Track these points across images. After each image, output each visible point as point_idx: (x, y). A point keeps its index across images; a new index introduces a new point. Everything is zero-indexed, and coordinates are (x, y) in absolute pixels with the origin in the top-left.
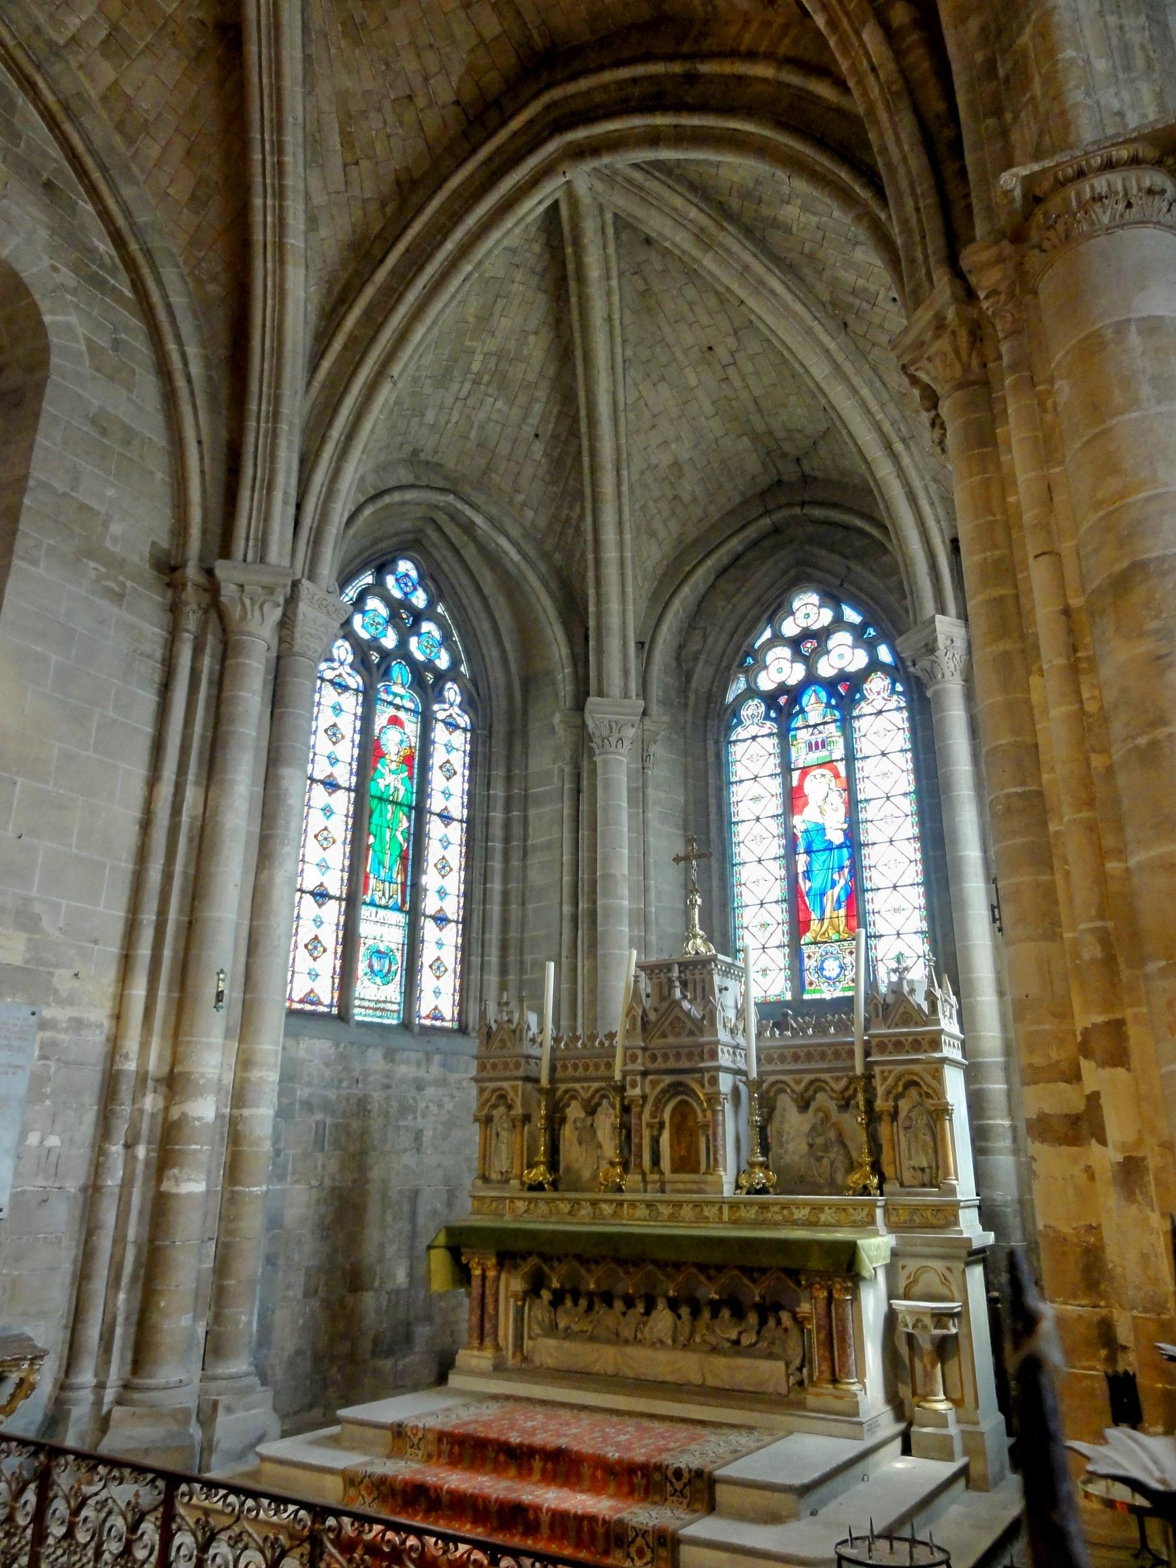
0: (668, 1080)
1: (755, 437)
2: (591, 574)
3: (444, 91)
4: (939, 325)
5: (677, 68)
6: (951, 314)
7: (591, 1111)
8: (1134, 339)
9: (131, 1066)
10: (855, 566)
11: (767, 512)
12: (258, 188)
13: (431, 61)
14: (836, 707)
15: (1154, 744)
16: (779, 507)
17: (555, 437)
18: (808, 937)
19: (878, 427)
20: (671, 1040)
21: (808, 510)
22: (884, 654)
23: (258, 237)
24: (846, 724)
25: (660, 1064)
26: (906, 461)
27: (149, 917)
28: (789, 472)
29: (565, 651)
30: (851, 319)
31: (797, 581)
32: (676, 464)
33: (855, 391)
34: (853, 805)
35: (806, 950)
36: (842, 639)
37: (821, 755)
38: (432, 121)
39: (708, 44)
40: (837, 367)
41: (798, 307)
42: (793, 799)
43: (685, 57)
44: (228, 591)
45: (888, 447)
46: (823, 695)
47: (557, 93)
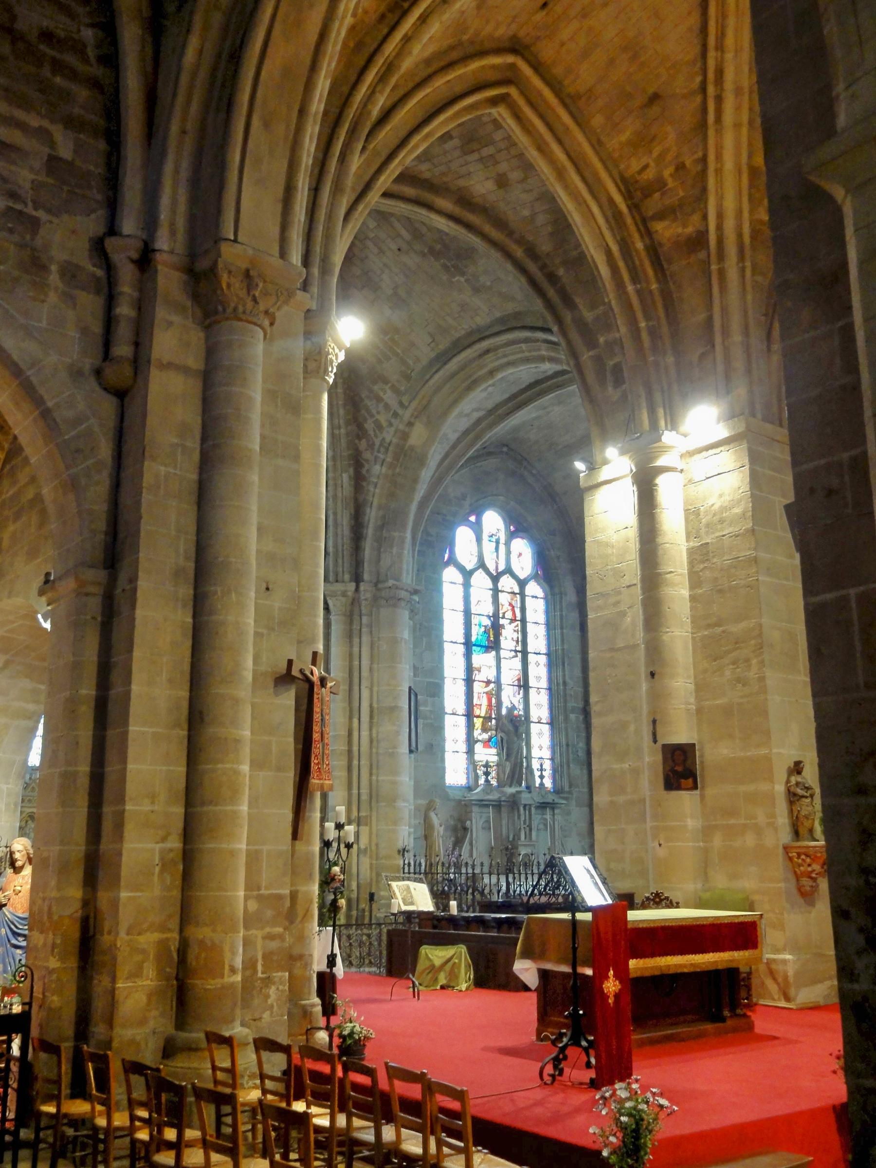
4: (344, 594)
6: (350, 594)
8: (403, 644)
15: (393, 753)
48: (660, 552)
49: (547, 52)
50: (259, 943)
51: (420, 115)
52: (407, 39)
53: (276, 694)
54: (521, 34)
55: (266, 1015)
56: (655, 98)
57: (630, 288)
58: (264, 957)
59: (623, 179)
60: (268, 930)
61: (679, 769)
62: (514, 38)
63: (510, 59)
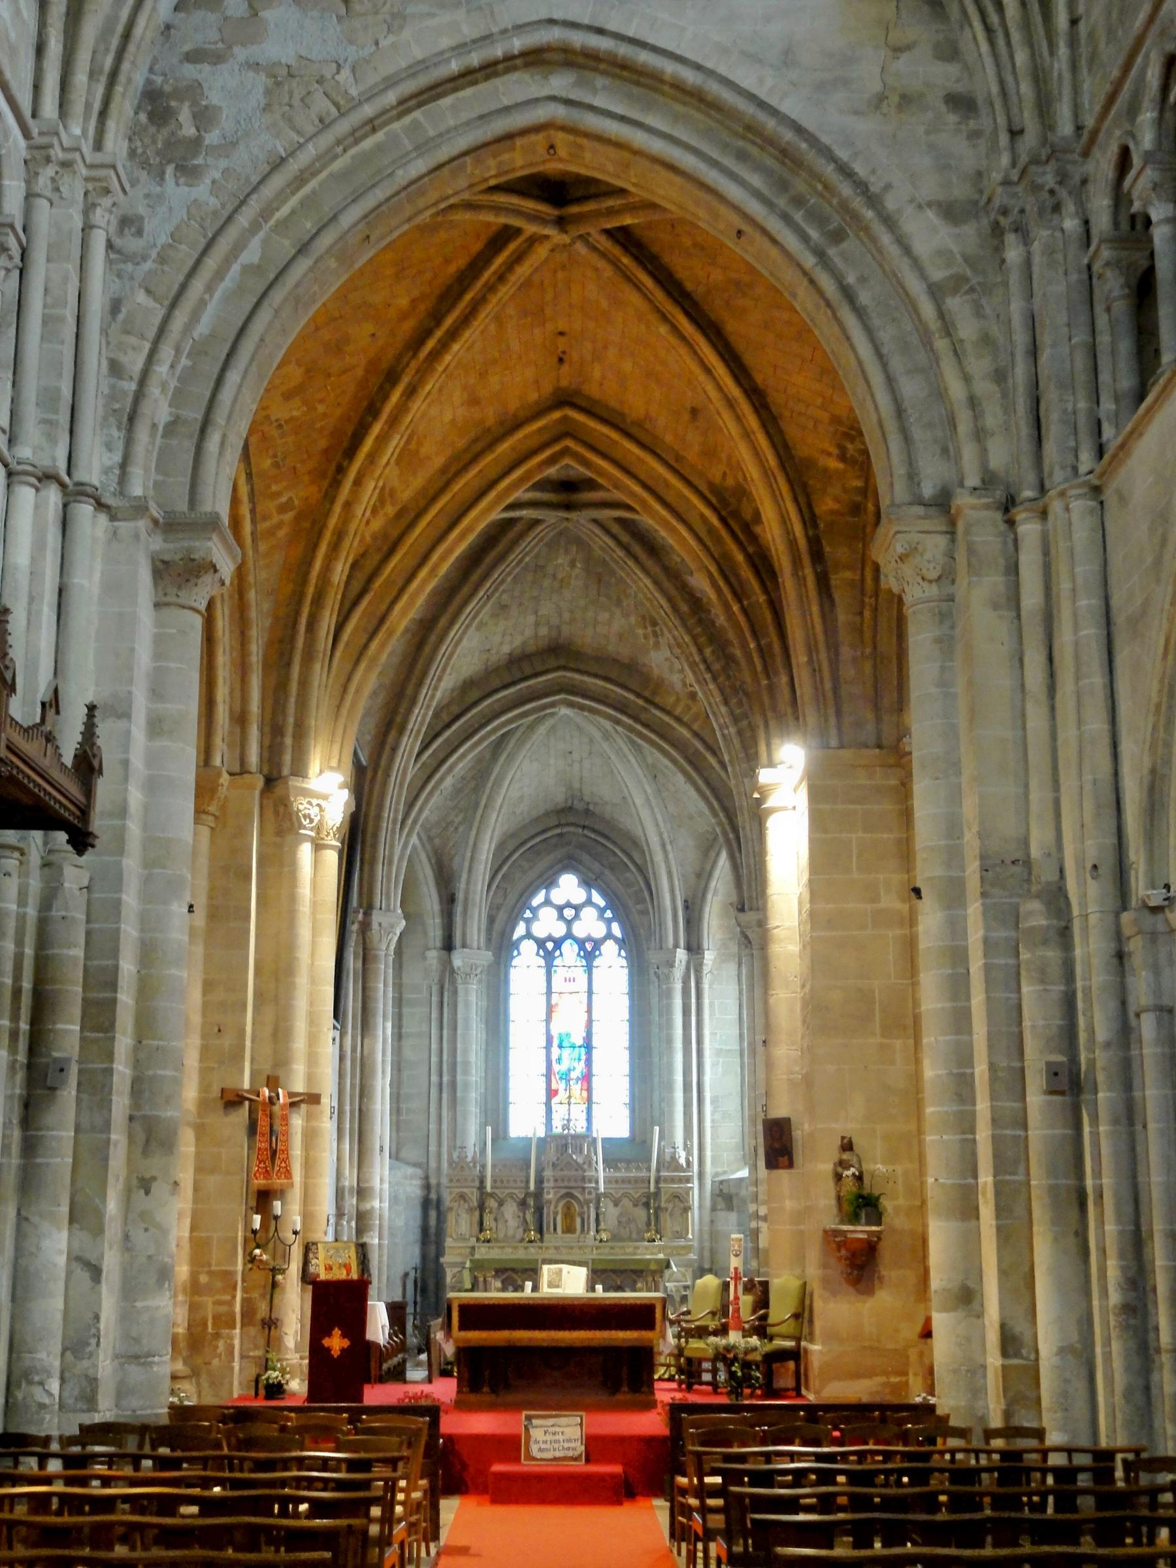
0: (564, 1191)
1: (570, 787)
2: (467, 864)
3: (506, 649)
5: (640, 702)
7: (501, 1204)
9: (347, 1184)
10: (607, 872)
11: (557, 826)
12: (419, 705)
13: (508, 638)
14: (584, 957)
16: (568, 824)
17: (463, 778)
18: (555, 1100)
19: (661, 835)
20: (566, 1173)
21: (586, 832)
22: (616, 929)
23: (410, 727)
24: (589, 969)
25: (560, 1184)
26: (671, 856)
27: (348, 1108)
28: (579, 806)
29: (437, 907)
30: (659, 776)
31: (566, 869)
32: (522, 797)
33: (653, 812)
34: (590, 1023)
35: (554, 1107)
36: (589, 913)
37: (571, 987)
38: (494, 658)
39: (657, 700)
40: (648, 799)
41: (639, 771)
42: (550, 1009)
43: (647, 700)
44: (375, 926)
45: (663, 846)
46: (576, 947)
47: (569, 674)
48: (769, 905)
49: (592, 390)
50: (210, 1306)
51: (443, 524)
52: (348, 505)
53: (226, 1114)
54: (564, 383)
55: (216, 1362)
56: (694, 412)
57: (736, 608)
58: (214, 1318)
59: (711, 485)
60: (217, 1297)
61: (776, 1145)
62: (558, 390)
63: (556, 415)
